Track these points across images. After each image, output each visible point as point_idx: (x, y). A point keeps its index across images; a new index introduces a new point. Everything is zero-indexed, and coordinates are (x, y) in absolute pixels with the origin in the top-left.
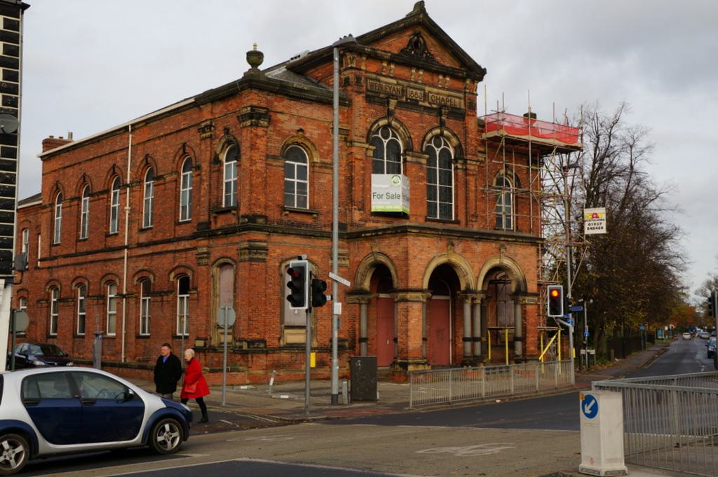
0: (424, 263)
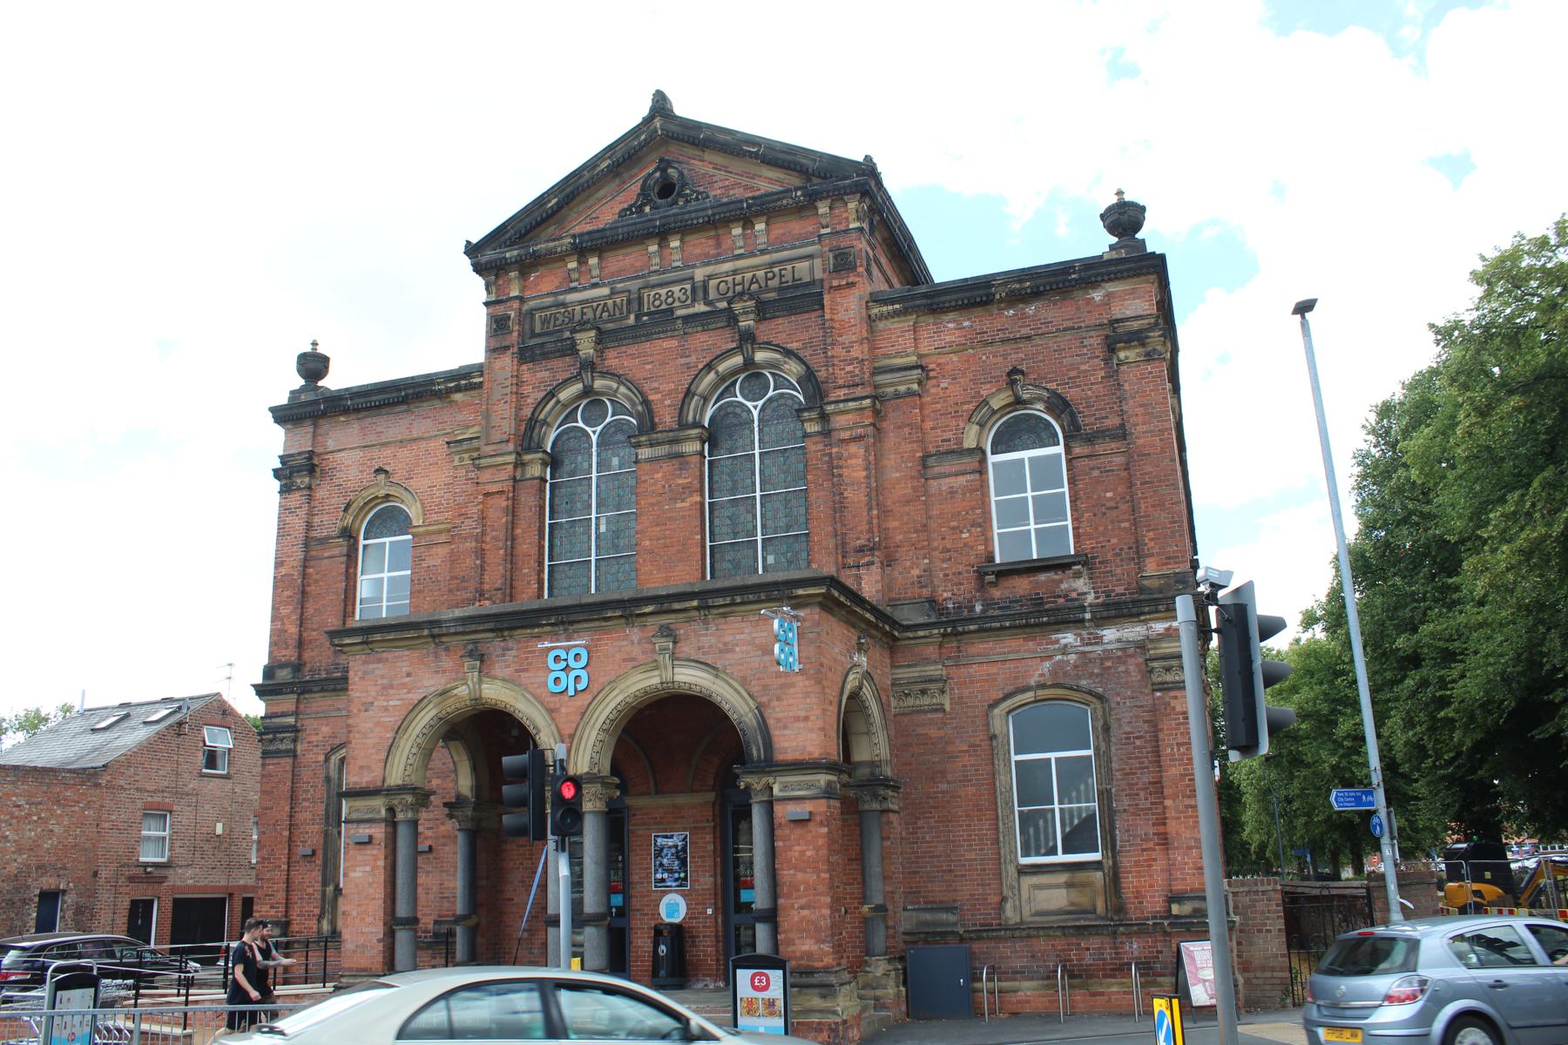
0: (392, 719)
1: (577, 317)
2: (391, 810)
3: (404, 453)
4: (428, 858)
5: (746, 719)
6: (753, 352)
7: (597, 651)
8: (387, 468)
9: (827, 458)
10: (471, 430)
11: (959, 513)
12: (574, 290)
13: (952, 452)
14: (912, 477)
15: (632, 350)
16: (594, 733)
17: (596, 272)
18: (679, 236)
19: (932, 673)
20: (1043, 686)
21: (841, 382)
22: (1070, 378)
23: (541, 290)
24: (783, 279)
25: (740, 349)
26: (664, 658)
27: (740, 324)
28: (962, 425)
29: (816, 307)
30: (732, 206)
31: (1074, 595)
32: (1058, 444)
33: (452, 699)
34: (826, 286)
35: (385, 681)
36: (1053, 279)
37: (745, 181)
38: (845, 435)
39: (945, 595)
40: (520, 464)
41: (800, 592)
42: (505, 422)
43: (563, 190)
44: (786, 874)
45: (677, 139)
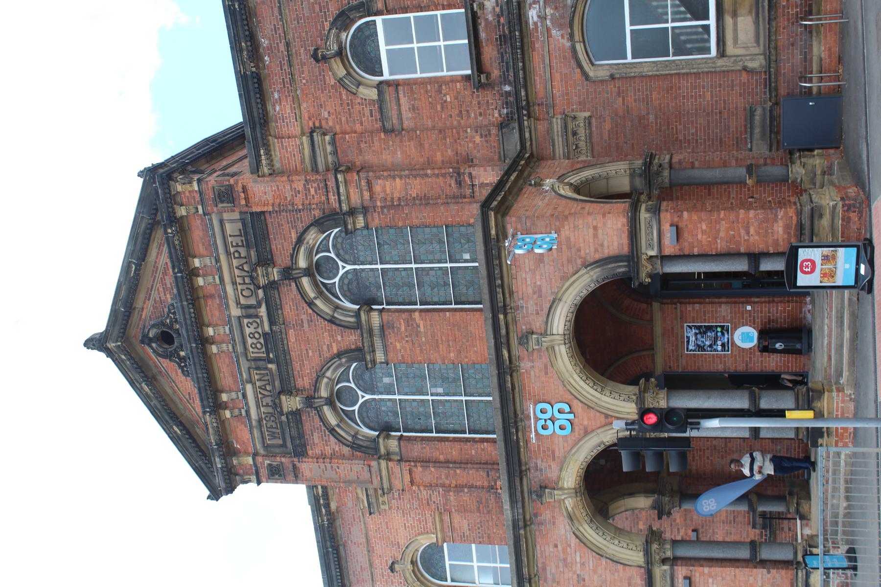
0: (591, 560)
1: (270, 410)
2: (664, 561)
3: (378, 549)
4: (702, 532)
5: (595, 277)
6: (299, 269)
7: (539, 395)
8: (390, 563)
9: (385, 210)
10: (360, 495)
11: (430, 103)
12: (248, 412)
13: (381, 109)
14: (401, 141)
15: (296, 365)
16: (604, 398)
17: (234, 396)
18: (205, 328)
19: (559, 126)
20: (572, 36)
21: (324, 198)
22: (321, 11)
23: (248, 439)
24: (240, 244)
25: (296, 280)
26: (545, 342)
27: (276, 279)
28: (359, 100)
29: (263, 217)
30: (180, 285)
31: (498, 9)
32: (375, 21)
33: (576, 512)
34: (245, 209)
35: (561, 565)
36: (239, 23)
37: (159, 275)
38: (366, 195)
39: (496, 115)
40: (388, 457)
41: (493, 232)
42: (354, 468)
43: (167, 422)
44: (721, 245)
45: (125, 329)
